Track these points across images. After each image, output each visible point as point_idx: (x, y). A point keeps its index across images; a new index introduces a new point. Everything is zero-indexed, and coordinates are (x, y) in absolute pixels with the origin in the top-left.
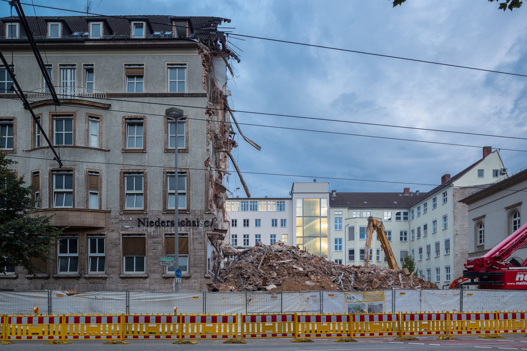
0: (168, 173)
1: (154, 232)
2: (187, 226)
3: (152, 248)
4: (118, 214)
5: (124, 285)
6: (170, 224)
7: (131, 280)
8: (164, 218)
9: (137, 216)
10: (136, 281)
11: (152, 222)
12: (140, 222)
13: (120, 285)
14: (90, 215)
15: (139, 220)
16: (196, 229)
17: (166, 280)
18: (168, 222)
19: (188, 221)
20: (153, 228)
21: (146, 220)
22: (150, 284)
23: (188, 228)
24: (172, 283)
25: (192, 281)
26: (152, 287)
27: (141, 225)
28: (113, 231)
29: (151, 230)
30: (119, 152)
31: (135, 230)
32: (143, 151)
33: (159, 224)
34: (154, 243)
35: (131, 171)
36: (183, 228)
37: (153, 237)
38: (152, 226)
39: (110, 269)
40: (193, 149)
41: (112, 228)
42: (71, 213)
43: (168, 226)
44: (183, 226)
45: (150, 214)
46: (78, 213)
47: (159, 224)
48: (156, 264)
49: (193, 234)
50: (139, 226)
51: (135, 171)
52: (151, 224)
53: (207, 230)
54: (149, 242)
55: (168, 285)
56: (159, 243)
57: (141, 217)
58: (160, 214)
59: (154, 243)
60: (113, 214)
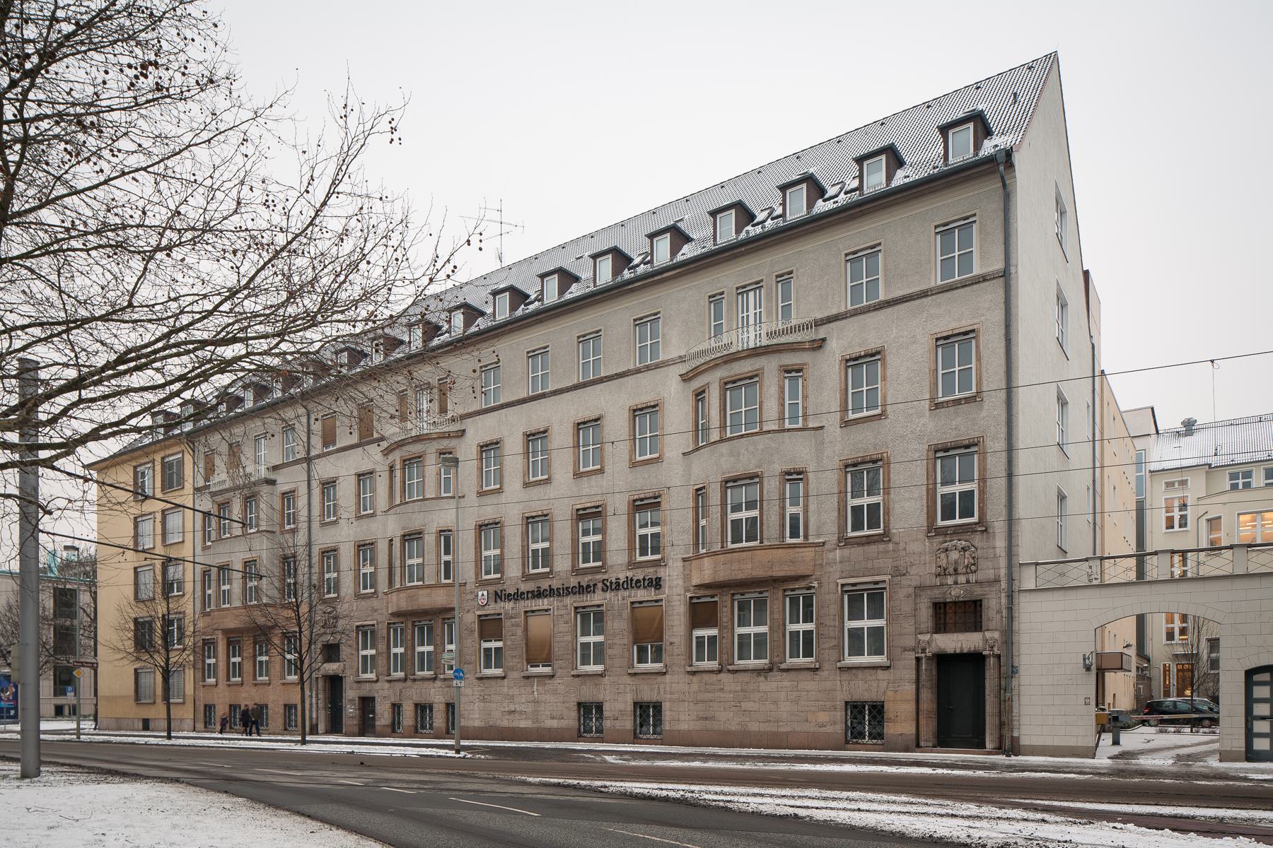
0: (528, 518)
1: (513, 608)
2: (550, 596)
3: (510, 633)
4: (474, 587)
5: (480, 688)
6: (530, 595)
7: (489, 681)
8: (524, 587)
9: (492, 589)
10: (493, 682)
11: (510, 595)
12: (498, 596)
13: (476, 689)
14: (442, 591)
15: (496, 593)
16: (561, 602)
17: (527, 681)
18: (528, 592)
19: (551, 589)
20: (511, 604)
21: (503, 593)
22: (508, 687)
23: (552, 599)
24: (533, 686)
25: (557, 681)
26: (511, 693)
27: (499, 600)
28: (468, 611)
29: (509, 606)
30: (474, 495)
31: (493, 608)
32: (547, 481)
33: (518, 596)
34: (513, 625)
35: (486, 522)
36: (545, 600)
37: (512, 618)
38: (510, 600)
39: (466, 666)
40: (557, 476)
41: (468, 608)
42: (421, 592)
43: (528, 598)
44: (546, 596)
45: (508, 583)
46: (428, 591)
47: (518, 596)
48: (515, 656)
49: (558, 609)
50: (496, 601)
51: (491, 521)
52: (509, 597)
53: (575, 602)
54: (507, 624)
55: (528, 689)
56: (518, 625)
57: (499, 588)
58: (519, 582)
59: (513, 625)
60: (468, 587)
